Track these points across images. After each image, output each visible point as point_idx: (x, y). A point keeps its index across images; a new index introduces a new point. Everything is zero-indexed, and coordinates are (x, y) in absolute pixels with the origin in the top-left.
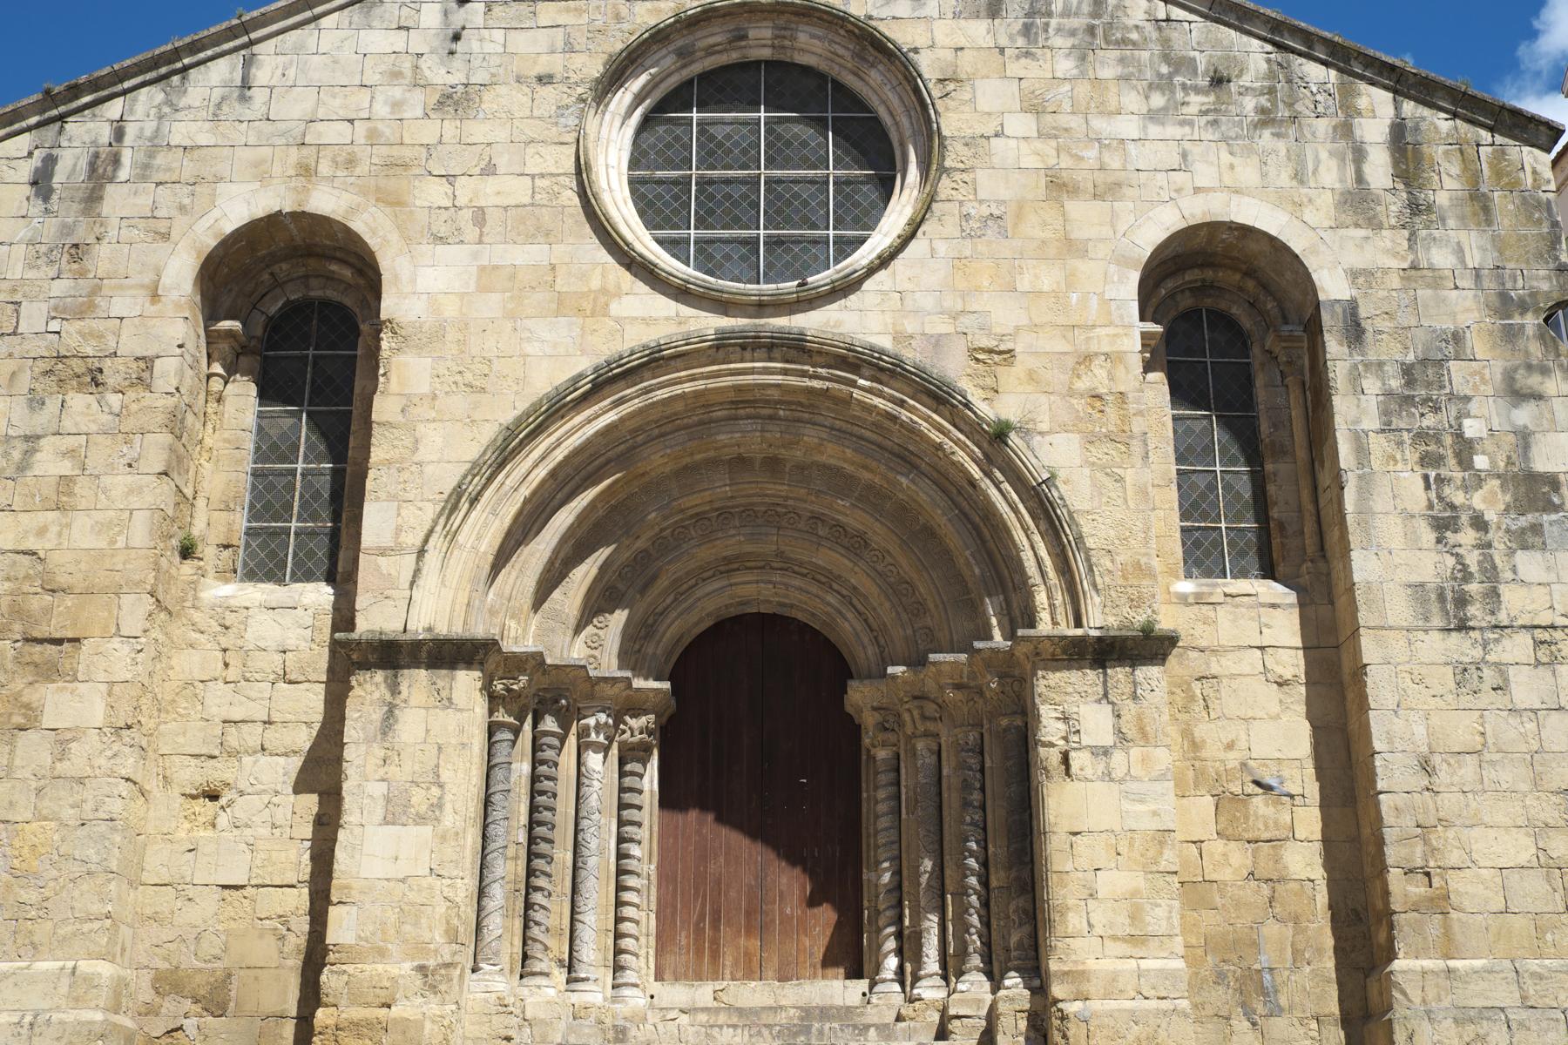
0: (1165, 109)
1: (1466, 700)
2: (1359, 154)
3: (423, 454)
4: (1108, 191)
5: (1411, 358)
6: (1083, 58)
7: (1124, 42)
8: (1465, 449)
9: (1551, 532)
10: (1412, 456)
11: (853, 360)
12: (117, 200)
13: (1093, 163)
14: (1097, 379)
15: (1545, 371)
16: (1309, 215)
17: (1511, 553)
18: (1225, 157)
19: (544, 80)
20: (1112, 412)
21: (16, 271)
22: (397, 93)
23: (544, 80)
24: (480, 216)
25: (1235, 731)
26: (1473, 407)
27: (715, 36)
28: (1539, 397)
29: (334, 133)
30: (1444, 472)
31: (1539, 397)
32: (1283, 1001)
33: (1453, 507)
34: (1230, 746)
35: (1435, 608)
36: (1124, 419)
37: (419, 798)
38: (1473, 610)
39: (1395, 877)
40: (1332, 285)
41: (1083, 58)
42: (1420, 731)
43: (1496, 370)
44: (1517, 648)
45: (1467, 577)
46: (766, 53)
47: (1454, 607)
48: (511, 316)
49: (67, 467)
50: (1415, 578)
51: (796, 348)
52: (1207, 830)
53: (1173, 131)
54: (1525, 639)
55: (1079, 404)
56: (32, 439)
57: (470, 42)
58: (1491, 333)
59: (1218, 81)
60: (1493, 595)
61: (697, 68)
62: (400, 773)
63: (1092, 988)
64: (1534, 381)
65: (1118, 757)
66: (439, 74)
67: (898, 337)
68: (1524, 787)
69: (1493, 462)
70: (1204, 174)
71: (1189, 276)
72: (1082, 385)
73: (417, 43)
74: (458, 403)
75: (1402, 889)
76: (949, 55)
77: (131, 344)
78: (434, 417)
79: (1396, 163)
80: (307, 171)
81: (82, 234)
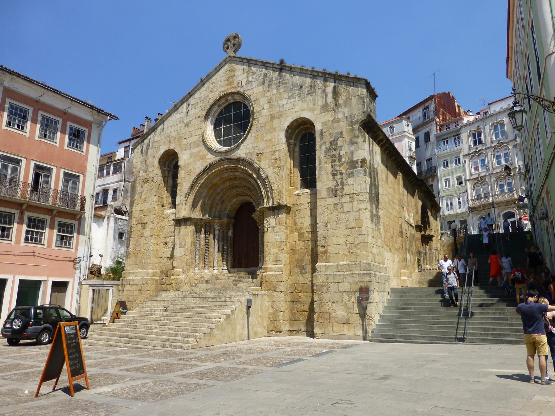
0: (291, 96)
1: (336, 211)
2: (326, 96)
3: (184, 187)
4: (280, 116)
5: (332, 139)
6: (278, 89)
7: (285, 83)
8: (340, 157)
9: (355, 173)
10: (330, 161)
11: (239, 160)
12: (150, 152)
13: (278, 111)
14: (277, 155)
15: (358, 137)
16: (316, 112)
17: (347, 179)
18: (301, 103)
19: (199, 117)
20: (278, 162)
21: (140, 166)
22: (180, 125)
23: (199, 117)
24: (190, 145)
25: (303, 220)
26: (343, 148)
27: (223, 101)
28: (356, 143)
29: (173, 134)
30: (336, 163)
31: (356, 143)
32: (307, 271)
33: (336, 171)
34: (301, 223)
35: (331, 193)
36: (280, 163)
37: (183, 243)
38: (338, 192)
39: (319, 247)
40: (318, 127)
41: (278, 89)
42: (326, 218)
43: (348, 139)
44: (346, 199)
45: (338, 185)
46: (232, 101)
47: (334, 192)
48: (194, 162)
49: (145, 196)
50: (328, 187)
51: (230, 160)
52: (297, 239)
53: (292, 100)
54: (348, 197)
55: (273, 161)
56: (142, 192)
57: (190, 113)
58: (348, 131)
59: (301, 87)
60: (343, 188)
61: (222, 107)
62: (181, 239)
63: (268, 270)
64: (355, 140)
65: (275, 228)
66: (186, 120)
67: (246, 154)
68: (344, 228)
69: (345, 160)
70: (297, 108)
71: (302, 127)
72: (273, 157)
73: (183, 116)
74: (187, 178)
75: (320, 250)
76: (255, 95)
77: (151, 176)
78: (185, 181)
79: (333, 97)
80: (170, 141)
81: (146, 159)
